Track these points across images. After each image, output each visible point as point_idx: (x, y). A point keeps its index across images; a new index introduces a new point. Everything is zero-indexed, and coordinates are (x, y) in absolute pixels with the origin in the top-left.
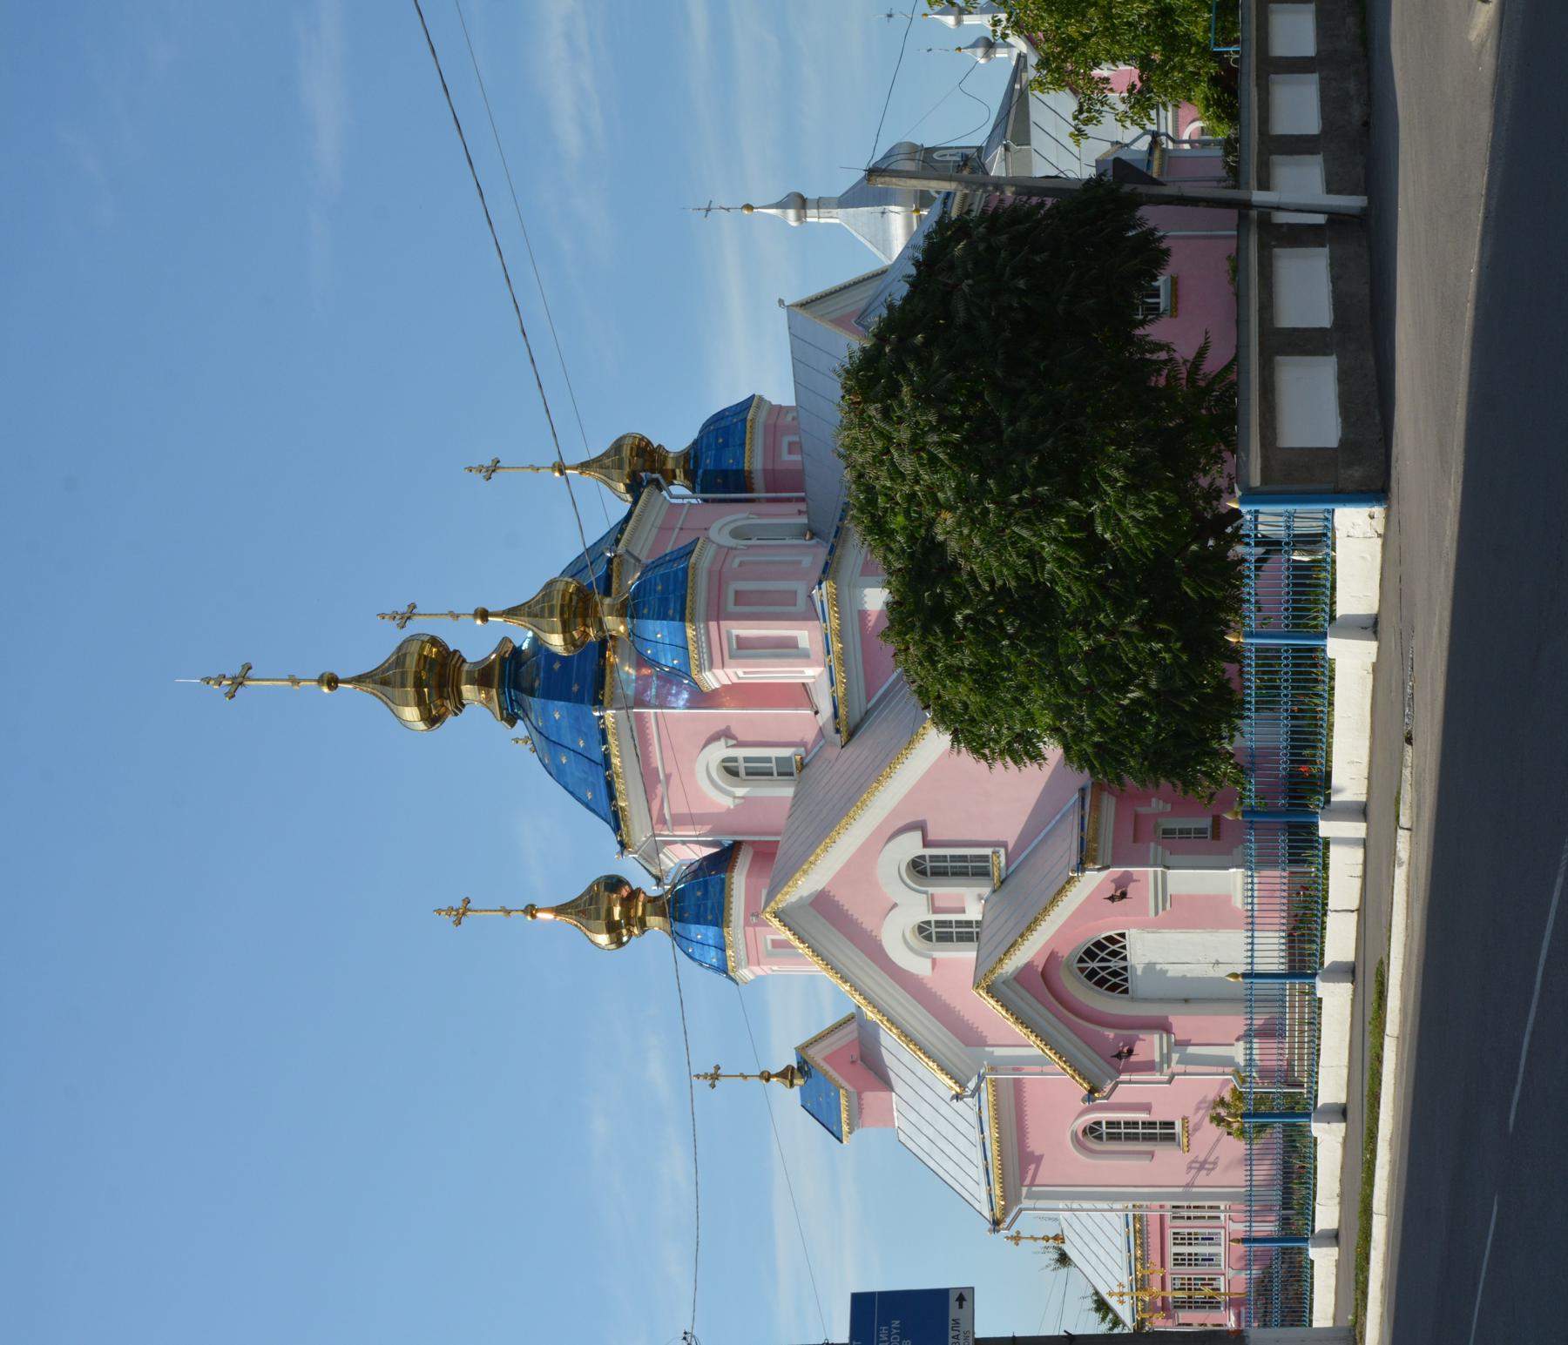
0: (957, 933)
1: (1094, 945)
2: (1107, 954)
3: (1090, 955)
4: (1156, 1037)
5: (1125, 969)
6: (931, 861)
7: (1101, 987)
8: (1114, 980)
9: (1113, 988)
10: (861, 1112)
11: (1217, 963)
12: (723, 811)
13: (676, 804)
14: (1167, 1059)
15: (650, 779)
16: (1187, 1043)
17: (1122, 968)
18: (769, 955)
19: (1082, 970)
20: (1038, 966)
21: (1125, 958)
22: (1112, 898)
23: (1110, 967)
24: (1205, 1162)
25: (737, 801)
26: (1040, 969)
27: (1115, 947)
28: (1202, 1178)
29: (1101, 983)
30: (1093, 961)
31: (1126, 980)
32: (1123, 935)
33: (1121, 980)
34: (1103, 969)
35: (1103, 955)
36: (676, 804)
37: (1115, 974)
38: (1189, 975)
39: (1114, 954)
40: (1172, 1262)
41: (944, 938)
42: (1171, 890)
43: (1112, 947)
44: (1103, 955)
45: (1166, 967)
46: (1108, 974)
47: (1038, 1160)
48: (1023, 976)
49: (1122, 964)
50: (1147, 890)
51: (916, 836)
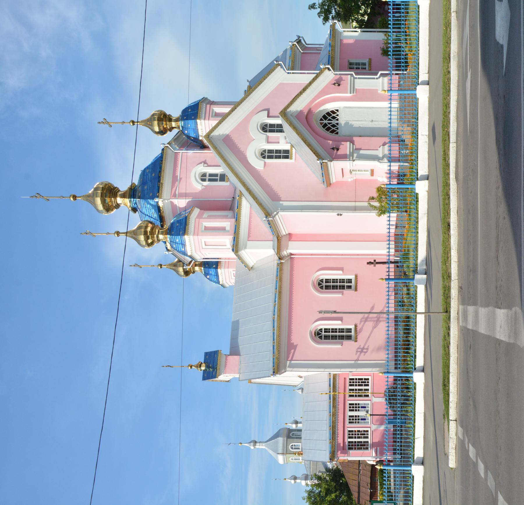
0: (275, 155)
1: (326, 114)
2: (331, 118)
3: (325, 117)
4: (348, 143)
5: (337, 124)
6: (268, 153)
7: (328, 131)
8: (333, 128)
9: (333, 132)
10: (225, 366)
11: (372, 121)
12: (198, 192)
13: (181, 188)
14: (352, 154)
15: (175, 179)
16: (360, 149)
17: (336, 124)
18: (202, 232)
19: (321, 124)
20: (305, 113)
21: (337, 120)
22: (334, 84)
23: (332, 123)
24: (363, 348)
25: (203, 187)
26: (305, 114)
27: (334, 115)
28: (362, 357)
29: (328, 129)
30: (326, 120)
31: (337, 129)
32: (337, 110)
33: (336, 129)
34: (329, 123)
35: (329, 118)
36: (181, 188)
37: (334, 126)
38: (361, 126)
39: (334, 118)
40: (348, 421)
41: (270, 157)
42: (356, 87)
43: (333, 115)
44: (329, 118)
45: (353, 123)
46: (331, 126)
47: (295, 347)
48: (299, 115)
49: (337, 122)
50: (348, 83)
51: (266, 112)
